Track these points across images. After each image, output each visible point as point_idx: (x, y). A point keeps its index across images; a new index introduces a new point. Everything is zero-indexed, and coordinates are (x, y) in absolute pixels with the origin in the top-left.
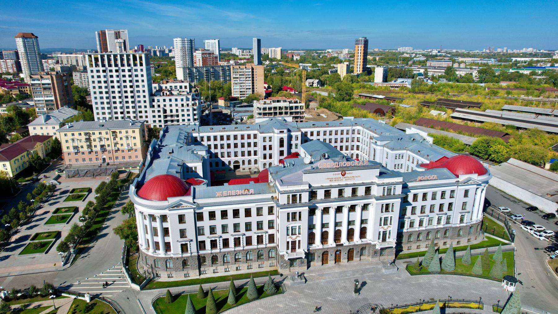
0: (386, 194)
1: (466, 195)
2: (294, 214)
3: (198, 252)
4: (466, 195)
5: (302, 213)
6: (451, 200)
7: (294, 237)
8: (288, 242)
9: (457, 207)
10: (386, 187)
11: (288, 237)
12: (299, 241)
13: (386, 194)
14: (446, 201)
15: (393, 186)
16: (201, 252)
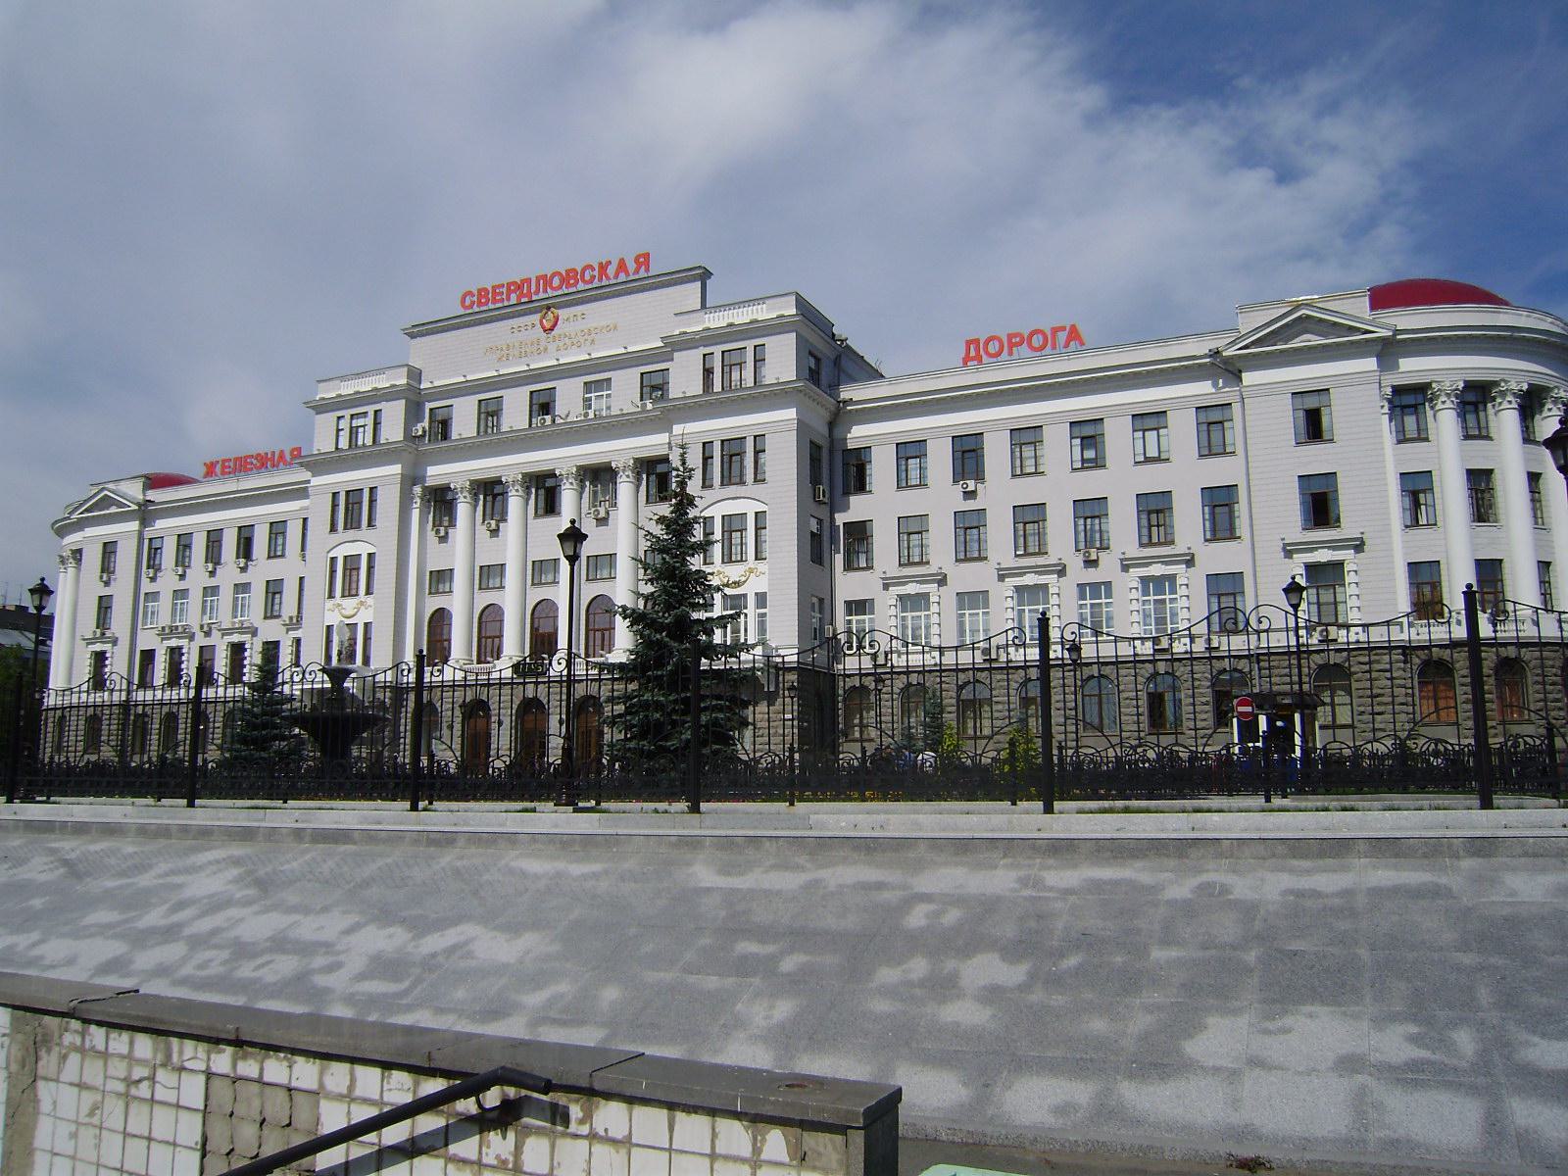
0: (717, 387)
1: (1313, 427)
2: (353, 496)
3: (129, 692)
4: (1313, 427)
5: (380, 492)
6: (1219, 472)
7: (350, 604)
8: (329, 628)
9: (1274, 510)
10: (717, 350)
11: (329, 604)
12: (367, 625)
13: (717, 387)
14: (1186, 478)
15: (750, 345)
16: (140, 696)
